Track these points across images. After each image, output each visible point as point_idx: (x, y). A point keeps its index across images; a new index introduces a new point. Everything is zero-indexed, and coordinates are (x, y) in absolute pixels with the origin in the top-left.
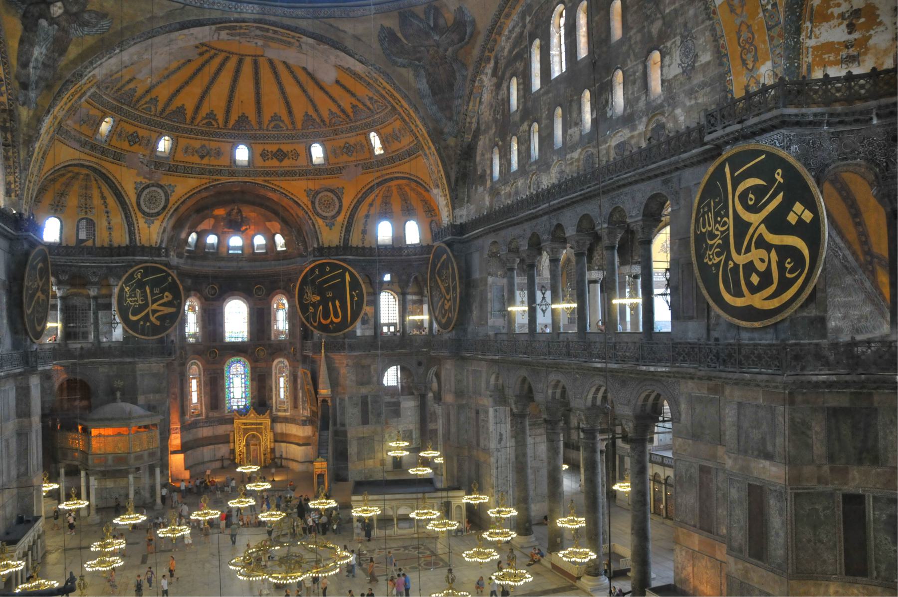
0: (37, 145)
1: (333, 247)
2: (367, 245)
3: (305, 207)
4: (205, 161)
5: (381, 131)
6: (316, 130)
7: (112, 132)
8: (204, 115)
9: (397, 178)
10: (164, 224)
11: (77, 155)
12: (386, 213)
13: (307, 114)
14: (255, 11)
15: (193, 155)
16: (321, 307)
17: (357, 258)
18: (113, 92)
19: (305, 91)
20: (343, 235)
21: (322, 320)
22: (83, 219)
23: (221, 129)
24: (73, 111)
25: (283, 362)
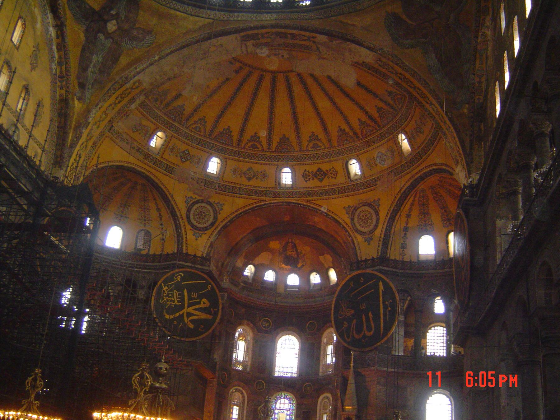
0: (85, 132)
1: (369, 260)
2: (406, 259)
3: (345, 226)
4: (251, 183)
5: (407, 129)
7: (166, 145)
8: (249, 138)
10: (212, 239)
11: (131, 159)
12: (426, 225)
13: (340, 130)
14: (272, 18)
15: (241, 177)
16: (355, 321)
17: (394, 270)
18: (162, 106)
19: (334, 103)
20: (380, 248)
21: (356, 336)
22: (142, 230)
23: (266, 151)
25: (327, 398)
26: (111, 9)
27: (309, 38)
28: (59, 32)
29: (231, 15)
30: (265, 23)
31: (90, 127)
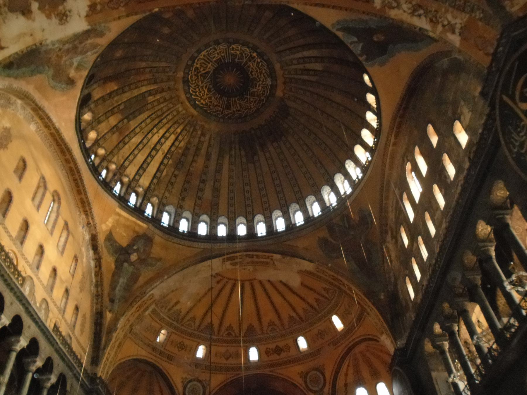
0: (115, 335)
6: (297, 327)
9: (358, 343)
13: (290, 317)
15: (221, 358)
18: (166, 311)
19: (285, 299)
24: (140, 319)
26: (134, 245)
27: (268, 257)
28: (97, 264)
29: (215, 245)
30: (238, 249)
31: (118, 332)
